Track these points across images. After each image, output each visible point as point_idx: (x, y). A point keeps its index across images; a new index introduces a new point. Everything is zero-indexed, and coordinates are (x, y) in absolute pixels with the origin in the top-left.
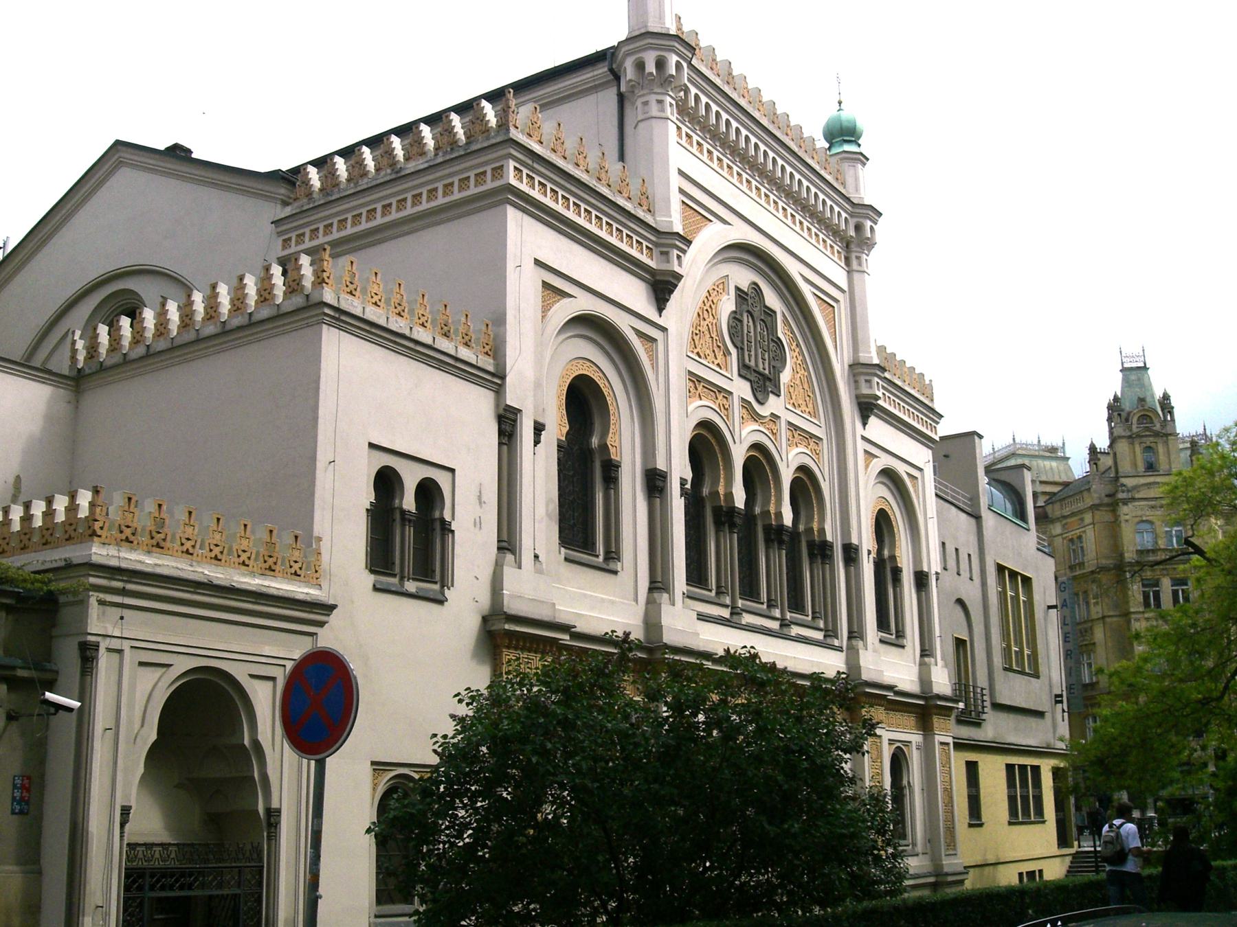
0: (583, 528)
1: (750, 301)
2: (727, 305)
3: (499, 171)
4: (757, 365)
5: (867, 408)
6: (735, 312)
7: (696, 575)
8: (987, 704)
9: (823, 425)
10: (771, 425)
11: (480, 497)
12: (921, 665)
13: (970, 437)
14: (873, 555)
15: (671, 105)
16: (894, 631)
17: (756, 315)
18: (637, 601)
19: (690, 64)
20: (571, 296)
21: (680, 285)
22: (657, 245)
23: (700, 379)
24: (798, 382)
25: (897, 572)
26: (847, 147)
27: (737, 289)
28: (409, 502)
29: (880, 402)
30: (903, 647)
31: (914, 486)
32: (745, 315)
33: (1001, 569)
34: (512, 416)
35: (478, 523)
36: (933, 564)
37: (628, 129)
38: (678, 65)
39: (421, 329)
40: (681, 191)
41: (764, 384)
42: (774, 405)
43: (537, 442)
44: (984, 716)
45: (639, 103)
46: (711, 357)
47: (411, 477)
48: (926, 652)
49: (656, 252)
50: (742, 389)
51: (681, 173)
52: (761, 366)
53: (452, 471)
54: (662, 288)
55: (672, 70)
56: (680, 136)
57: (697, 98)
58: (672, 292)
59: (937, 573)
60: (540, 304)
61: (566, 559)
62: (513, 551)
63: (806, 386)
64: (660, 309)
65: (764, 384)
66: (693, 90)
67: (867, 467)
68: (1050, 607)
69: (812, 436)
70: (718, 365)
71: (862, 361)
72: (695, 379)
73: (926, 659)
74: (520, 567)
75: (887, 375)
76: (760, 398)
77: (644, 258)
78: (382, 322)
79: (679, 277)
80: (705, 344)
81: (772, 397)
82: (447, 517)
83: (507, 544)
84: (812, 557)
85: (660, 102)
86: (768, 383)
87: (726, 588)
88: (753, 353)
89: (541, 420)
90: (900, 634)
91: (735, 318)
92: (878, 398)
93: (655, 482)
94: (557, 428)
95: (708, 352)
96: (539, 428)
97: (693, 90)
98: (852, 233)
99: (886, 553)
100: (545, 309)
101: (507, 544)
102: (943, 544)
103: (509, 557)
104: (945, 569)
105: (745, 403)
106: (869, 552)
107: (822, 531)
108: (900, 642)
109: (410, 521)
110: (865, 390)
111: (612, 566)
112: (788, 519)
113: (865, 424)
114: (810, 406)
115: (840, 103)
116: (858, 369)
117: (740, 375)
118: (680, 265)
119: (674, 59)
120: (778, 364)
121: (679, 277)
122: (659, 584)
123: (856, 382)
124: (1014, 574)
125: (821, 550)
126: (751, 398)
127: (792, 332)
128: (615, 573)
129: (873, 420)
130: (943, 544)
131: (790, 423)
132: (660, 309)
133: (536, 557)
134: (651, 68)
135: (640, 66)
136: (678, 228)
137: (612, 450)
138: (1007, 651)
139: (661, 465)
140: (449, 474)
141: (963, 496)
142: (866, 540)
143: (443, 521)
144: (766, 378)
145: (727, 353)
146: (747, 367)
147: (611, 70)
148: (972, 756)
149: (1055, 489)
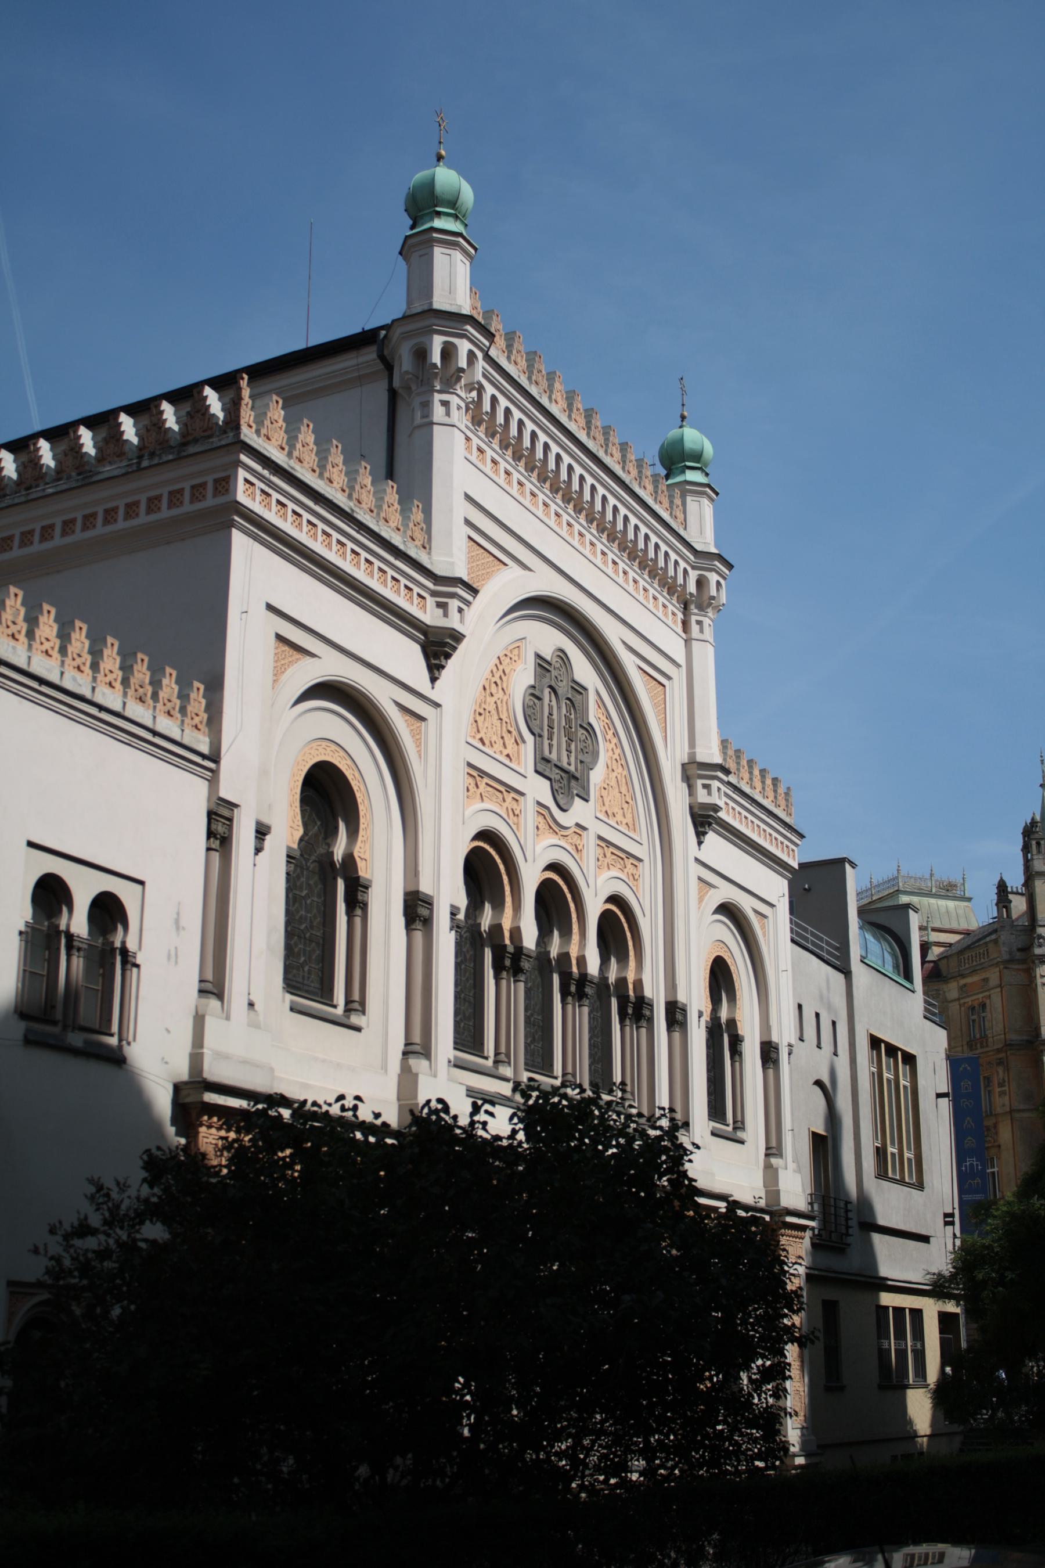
0: (314, 970)
1: (554, 673)
2: (523, 677)
3: (225, 484)
4: (559, 759)
5: (703, 820)
6: (533, 687)
7: (469, 1035)
8: (853, 1223)
9: (645, 841)
10: (576, 839)
11: (177, 922)
12: (768, 1167)
13: (837, 865)
14: (706, 1017)
15: (459, 408)
16: (560, 1074)
17: (560, 692)
18: (384, 1068)
19: (487, 358)
20: (313, 655)
21: (462, 648)
22: (434, 594)
23: (483, 774)
24: (613, 783)
25: (736, 1041)
26: (691, 476)
27: (538, 656)
28: (78, 923)
29: (722, 814)
30: (742, 1142)
31: (763, 927)
32: (547, 690)
33: (875, 1042)
34: (225, 812)
35: (173, 956)
36: (784, 1033)
37: (401, 438)
38: (471, 355)
39: (107, 690)
40: (468, 522)
41: (568, 783)
42: (579, 812)
43: (258, 850)
44: (850, 1240)
45: (416, 402)
46: (499, 746)
47: (84, 889)
48: (773, 1150)
49: (430, 601)
50: (539, 789)
51: (468, 497)
52: (565, 760)
53: (142, 883)
54: (438, 648)
55: (463, 363)
56: (468, 449)
57: (494, 400)
58: (448, 656)
59: (790, 1045)
60: (271, 664)
61: (292, 1009)
62: (220, 996)
63: (624, 790)
64: (433, 680)
65: (568, 783)
66: (490, 390)
67: (701, 900)
68: (939, 1096)
69: (630, 855)
70: (508, 756)
71: (700, 758)
72: (477, 772)
73: (774, 1161)
74: (228, 1018)
75: (732, 779)
76: (561, 803)
77: (414, 610)
78: (54, 678)
79: (457, 637)
80: (491, 728)
81: (577, 801)
82: (131, 945)
83: (213, 987)
85: (445, 404)
86: (573, 783)
87: (508, 1055)
88: (555, 742)
89: (266, 820)
90: (739, 1125)
91: (534, 694)
92: (716, 808)
93: (417, 910)
94: (288, 828)
95: (494, 738)
96: (262, 832)
97: (490, 390)
98: (692, 588)
99: (724, 1014)
100: (278, 672)
101: (213, 987)
102: (800, 1006)
103: (214, 1003)
104: (801, 1040)
106: (700, 1014)
107: (639, 984)
108: (740, 1134)
109: (79, 949)
110: (702, 797)
111: (355, 1019)
112: (593, 967)
113: (700, 843)
114: (629, 815)
116: (693, 771)
117: (536, 771)
118: (462, 621)
119: (464, 347)
120: (587, 758)
121: (457, 637)
122: (417, 1047)
123: (690, 787)
124: (892, 1050)
125: (637, 1010)
126: (549, 802)
127: (609, 716)
128: (358, 1029)
129: (711, 837)
130: (800, 1006)
131: (600, 838)
132: (433, 680)
133: (251, 1005)
134: (436, 358)
135: (422, 354)
136: (462, 573)
137: (360, 864)
138: (880, 1153)
139: (425, 887)
140: (139, 887)
141: (828, 943)
142: (696, 996)
143: (124, 952)
146: (548, 761)
147: (382, 358)
148: (831, 1294)
149: (953, 938)
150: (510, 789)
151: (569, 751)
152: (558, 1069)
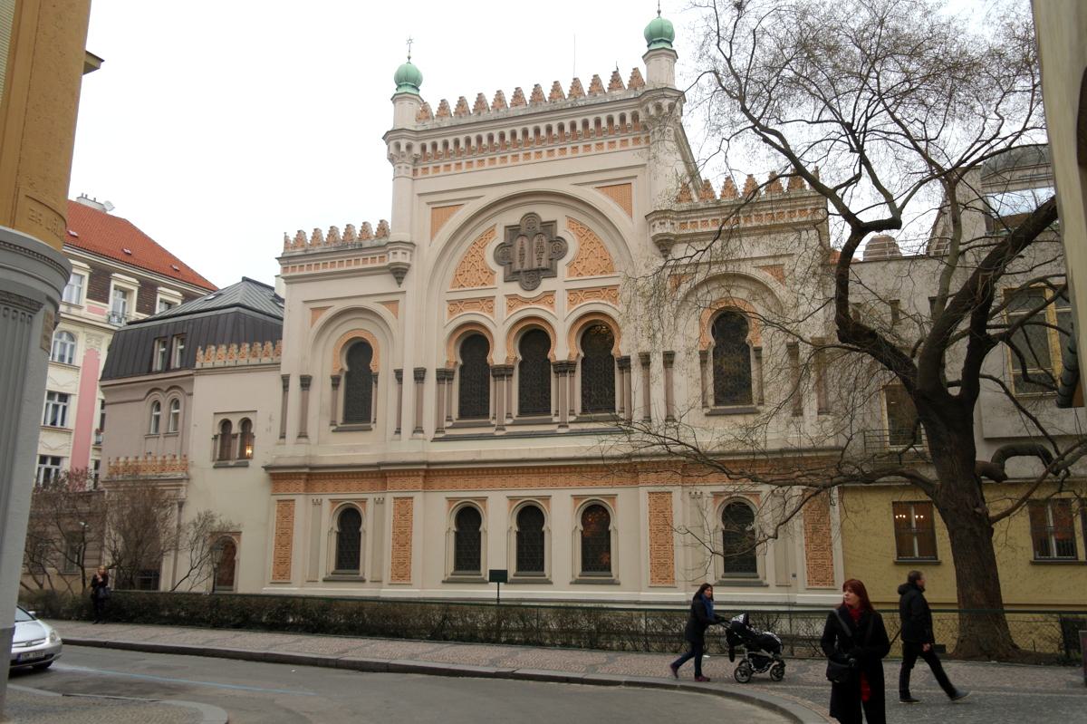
35: (269, 430)
39: (242, 360)
40: (428, 204)
42: (546, 284)
49: (386, 255)
53: (256, 411)
64: (400, 283)
69: (604, 288)
77: (377, 264)
84: (621, 368)
90: (761, 402)
105: (512, 298)
115: (659, 12)
125: (625, 363)
132: (400, 283)
144: (537, 270)
145: (493, 273)
146: (519, 272)
150: (483, 299)
151: (540, 259)
152: (553, 411)
